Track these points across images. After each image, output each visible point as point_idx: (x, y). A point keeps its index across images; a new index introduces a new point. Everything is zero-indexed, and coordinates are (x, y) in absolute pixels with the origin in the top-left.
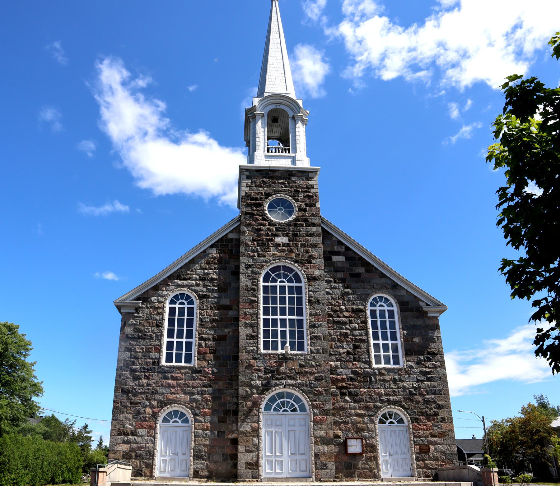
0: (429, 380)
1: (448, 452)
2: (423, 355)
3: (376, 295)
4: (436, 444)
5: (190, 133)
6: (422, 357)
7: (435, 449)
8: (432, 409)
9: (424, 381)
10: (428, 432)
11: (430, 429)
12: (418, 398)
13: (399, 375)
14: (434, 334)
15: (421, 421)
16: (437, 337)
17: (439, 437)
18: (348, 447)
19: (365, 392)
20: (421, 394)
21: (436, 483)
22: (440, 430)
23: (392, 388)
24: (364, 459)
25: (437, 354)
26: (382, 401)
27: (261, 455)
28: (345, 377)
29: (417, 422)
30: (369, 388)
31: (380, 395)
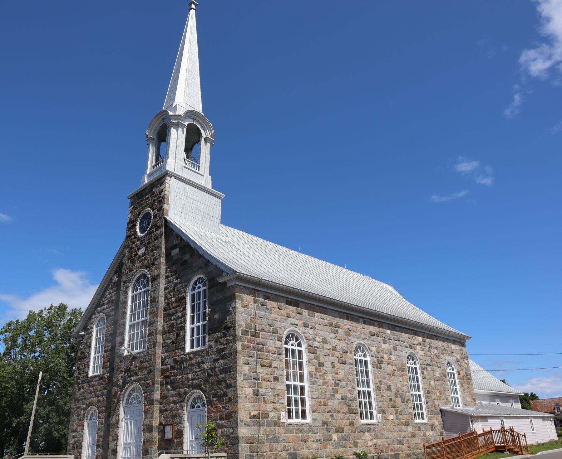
0: (223, 357)
1: (232, 435)
2: (220, 331)
3: (196, 278)
4: (223, 427)
5: (161, 185)
6: (219, 334)
7: (222, 432)
8: (222, 390)
9: (219, 359)
10: (218, 414)
11: (220, 412)
12: (213, 379)
13: (203, 357)
14: (231, 305)
15: (214, 403)
16: (233, 308)
17: (226, 419)
18: (166, 434)
19: (179, 379)
20: (216, 375)
21: (462, 333)
22: (227, 411)
23: (196, 372)
24: (175, 445)
25: (231, 327)
26: (189, 387)
27: (119, 444)
28: (169, 366)
29: (211, 405)
30: (182, 374)
31: (188, 380)
